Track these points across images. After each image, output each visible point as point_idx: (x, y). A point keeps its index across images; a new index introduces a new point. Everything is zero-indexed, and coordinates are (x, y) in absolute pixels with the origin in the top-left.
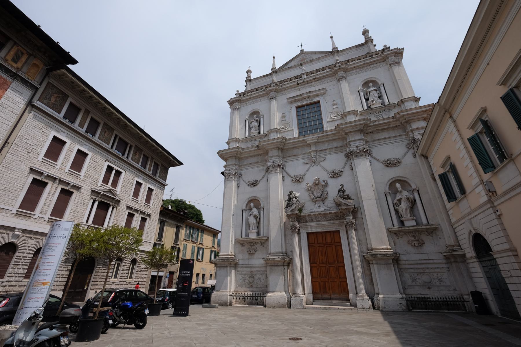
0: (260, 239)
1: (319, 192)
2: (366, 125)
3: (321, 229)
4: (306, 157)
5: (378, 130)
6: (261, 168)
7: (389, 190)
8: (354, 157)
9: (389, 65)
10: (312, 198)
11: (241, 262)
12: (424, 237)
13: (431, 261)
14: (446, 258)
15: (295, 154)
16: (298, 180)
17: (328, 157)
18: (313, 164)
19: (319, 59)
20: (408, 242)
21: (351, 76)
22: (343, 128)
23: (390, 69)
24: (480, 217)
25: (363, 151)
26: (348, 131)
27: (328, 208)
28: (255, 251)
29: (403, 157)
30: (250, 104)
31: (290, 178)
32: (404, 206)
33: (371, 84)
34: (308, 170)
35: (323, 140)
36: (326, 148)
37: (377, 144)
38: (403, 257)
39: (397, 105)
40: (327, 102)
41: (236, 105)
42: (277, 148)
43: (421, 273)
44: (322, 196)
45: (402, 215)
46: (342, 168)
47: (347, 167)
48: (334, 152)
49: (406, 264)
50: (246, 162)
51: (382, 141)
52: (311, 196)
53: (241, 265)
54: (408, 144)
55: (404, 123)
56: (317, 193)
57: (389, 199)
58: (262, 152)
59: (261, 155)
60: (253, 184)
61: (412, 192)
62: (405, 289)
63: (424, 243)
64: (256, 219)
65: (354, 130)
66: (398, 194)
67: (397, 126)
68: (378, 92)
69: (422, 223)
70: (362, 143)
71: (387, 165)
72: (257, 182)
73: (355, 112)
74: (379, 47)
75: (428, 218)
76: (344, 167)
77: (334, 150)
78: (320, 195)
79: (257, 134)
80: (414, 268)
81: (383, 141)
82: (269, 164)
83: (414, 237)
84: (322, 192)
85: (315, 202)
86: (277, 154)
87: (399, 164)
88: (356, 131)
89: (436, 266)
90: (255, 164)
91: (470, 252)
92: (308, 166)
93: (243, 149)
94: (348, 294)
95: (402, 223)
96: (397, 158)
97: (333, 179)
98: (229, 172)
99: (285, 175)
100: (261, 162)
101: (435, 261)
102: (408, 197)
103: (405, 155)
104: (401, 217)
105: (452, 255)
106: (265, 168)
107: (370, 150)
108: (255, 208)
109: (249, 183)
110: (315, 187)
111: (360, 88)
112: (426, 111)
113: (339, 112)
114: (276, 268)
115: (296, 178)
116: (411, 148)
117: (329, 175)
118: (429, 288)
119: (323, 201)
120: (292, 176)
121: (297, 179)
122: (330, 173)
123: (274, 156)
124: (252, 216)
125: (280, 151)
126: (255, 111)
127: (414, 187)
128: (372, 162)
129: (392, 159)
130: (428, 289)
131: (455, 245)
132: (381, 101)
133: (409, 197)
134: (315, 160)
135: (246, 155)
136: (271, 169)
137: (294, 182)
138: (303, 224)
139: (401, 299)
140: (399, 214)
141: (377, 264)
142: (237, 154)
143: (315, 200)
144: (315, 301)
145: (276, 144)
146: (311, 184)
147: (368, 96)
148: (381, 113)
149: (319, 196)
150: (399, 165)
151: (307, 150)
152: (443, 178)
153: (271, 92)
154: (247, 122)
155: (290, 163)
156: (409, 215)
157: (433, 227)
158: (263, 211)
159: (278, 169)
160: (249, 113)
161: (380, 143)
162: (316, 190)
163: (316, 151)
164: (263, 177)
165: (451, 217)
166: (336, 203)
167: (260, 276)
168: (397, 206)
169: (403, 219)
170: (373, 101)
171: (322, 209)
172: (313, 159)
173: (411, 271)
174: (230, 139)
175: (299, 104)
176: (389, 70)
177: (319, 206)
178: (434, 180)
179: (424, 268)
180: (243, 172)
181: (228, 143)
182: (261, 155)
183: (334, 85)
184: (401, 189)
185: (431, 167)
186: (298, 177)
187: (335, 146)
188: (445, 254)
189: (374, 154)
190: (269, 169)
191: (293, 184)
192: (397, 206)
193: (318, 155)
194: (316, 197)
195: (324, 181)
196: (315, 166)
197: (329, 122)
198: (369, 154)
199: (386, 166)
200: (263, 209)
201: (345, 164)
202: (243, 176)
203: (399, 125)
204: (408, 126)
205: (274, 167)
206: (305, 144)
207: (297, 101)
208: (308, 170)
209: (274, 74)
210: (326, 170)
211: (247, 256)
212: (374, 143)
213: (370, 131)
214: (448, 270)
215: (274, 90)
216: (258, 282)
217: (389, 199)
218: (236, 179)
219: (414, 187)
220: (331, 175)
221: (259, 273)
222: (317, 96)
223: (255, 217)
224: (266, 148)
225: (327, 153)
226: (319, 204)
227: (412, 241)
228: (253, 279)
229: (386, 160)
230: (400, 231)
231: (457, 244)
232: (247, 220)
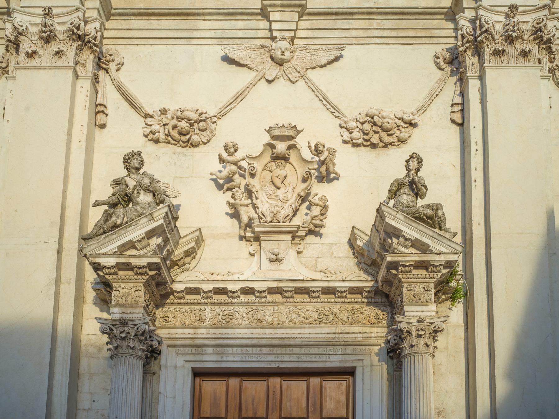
3: (271, 358)
4: (240, 34)
18: (272, 71)
31: (139, 121)
34: (240, 96)
46: (414, 110)
48: (387, 33)
76: (423, 109)
92: (246, 76)
115: (174, 122)
122: (353, 124)
137: (157, 141)
186: (179, 118)
196: (282, 83)
201: (434, 96)
208: (240, 96)
220: (356, 134)
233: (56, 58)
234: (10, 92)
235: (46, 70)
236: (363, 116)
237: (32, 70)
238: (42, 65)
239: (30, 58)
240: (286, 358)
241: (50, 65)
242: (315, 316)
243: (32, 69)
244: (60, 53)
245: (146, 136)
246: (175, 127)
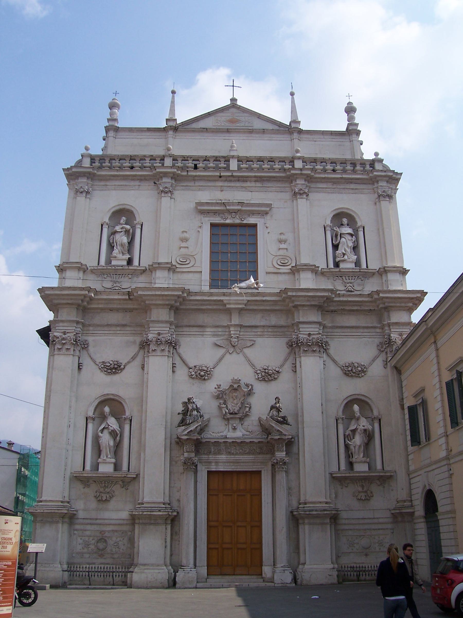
0: (123, 476)
1: (237, 404)
2: (328, 299)
3: (233, 467)
4: (220, 333)
5: (344, 310)
6: (131, 338)
7: (343, 415)
8: (302, 350)
9: (376, 195)
10: (224, 412)
11: (81, 514)
12: (374, 488)
13: (376, 521)
14: (394, 516)
15: (200, 323)
16: (201, 376)
17: (259, 340)
18: (231, 350)
19: (264, 131)
20: (354, 493)
21: (317, 192)
22: (293, 296)
23: (377, 203)
24: (436, 472)
25: (317, 344)
26: (299, 303)
27: (248, 433)
28: (111, 498)
29: (371, 364)
30: (115, 190)
32: (358, 440)
33: (345, 221)
34: (221, 359)
35: (255, 308)
36: (258, 324)
37: (338, 334)
38: (344, 515)
39: (378, 271)
40: (268, 233)
41: (83, 182)
42: (168, 305)
43: (360, 536)
44: (241, 411)
45: (353, 454)
47: (288, 366)
48: (270, 333)
49: (345, 524)
50: (97, 320)
51: (346, 330)
52: (223, 409)
53: (81, 521)
54: (381, 343)
55: (382, 308)
56: (233, 405)
57: (341, 427)
58: (135, 307)
59: (131, 310)
60: (111, 369)
61: (372, 420)
62: (338, 557)
63: (373, 496)
64: (115, 439)
65: (308, 303)
66: (353, 422)
67: (370, 310)
68: (354, 240)
69: (376, 469)
70: (317, 330)
71: (347, 372)
72: (120, 366)
73: (314, 270)
74: (368, 155)
75: (384, 461)
76: (282, 366)
77: (270, 330)
78: (238, 408)
79: (125, 263)
80: (354, 529)
81: (349, 330)
82: (150, 336)
83: (363, 487)
84: (242, 403)
85: (228, 419)
86: (167, 319)
87: (363, 374)
88: (311, 306)
89: (380, 526)
90: (118, 328)
91: (420, 510)
92: (222, 351)
93: (96, 292)
94: (261, 566)
95: (351, 465)
96: (363, 364)
97: (263, 383)
98: (64, 336)
99: (178, 361)
100: (130, 326)
101: (381, 520)
102: (365, 427)
103: (374, 360)
104: (351, 456)
105: (401, 513)
106: (138, 339)
107: (327, 342)
108: (113, 416)
109: (102, 366)
110: (231, 394)
111: (328, 222)
112: (412, 298)
113: (288, 258)
114: (152, 527)
115: (199, 372)
116: (383, 351)
117: (257, 376)
118: (366, 555)
119: (241, 419)
120: (191, 365)
121: (199, 373)
122: (259, 372)
123: (162, 322)
124: (106, 431)
125: (172, 312)
126: (124, 209)
127: (376, 413)
128: (326, 363)
129: (356, 365)
130: (365, 557)
131: (408, 500)
132: (356, 257)
133: (367, 428)
134: (236, 343)
135: (100, 306)
136: (152, 347)
137: (193, 378)
138: (204, 457)
139: (331, 570)
140: (350, 452)
141: (310, 524)
142: (82, 301)
143: (229, 416)
144: (209, 577)
145: (168, 298)
146: (225, 386)
147: (337, 242)
148: (353, 281)
149: (236, 411)
150: (362, 376)
151: (223, 320)
152: (413, 410)
153: (164, 176)
154: (105, 230)
155: (188, 339)
156: (362, 455)
157: (387, 474)
158: (129, 425)
159: (167, 349)
160: (112, 211)
161: (343, 334)
162: (231, 400)
163: (241, 326)
164: (133, 358)
165: (410, 462)
166: (261, 425)
167: (118, 539)
168: (348, 440)
169: (354, 460)
170: (344, 254)
171: (238, 434)
172: (234, 340)
173: (350, 533)
174: (67, 263)
175: (218, 220)
176: (376, 203)
177: (235, 429)
178: (403, 408)
179: (365, 530)
180: (90, 339)
181: (61, 269)
182: (131, 310)
183: (286, 202)
184: (359, 414)
185: (402, 388)
187: (273, 323)
188: (393, 512)
189: (331, 351)
190: (149, 345)
191: (191, 380)
192: (349, 439)
193: (241, 334)
194: (232, 411)
195: (247, 385)
197: (269, 273)
198: (325, 349)
199: (345, 374)
200: (129, 422)
201: (286, 360)
202: (91, 349)
203: (374, 310)
204: (386, 314)
205: (158, 342)
206: (221, 307)
207: (215, 213)
208: (221, 359)
209: (171, 133)
210: (253, 366)
211: (93, 504)
212: (335, 330)
213: (332, 308)
214: (392, 531)
215: (172, 175)
216: (114, 550)
217: (341, 427)
218: (77, 353)
219: (376, 413)
220: (260, 376)
221: (116, 534)
222: (252, 213)
223: (113, 434)
224: (147, 302)
225: (259, 333)
226: (235, 425)
227: (359, 492)
228: (104, 544)
229: (347, 364)
230: (346, 478)
231: (410, 499)
232: (96, 439)
236: (262, 369)
240: (238, 467)
242: (248, 451)
245: (190, 376)
246: (199, 373)
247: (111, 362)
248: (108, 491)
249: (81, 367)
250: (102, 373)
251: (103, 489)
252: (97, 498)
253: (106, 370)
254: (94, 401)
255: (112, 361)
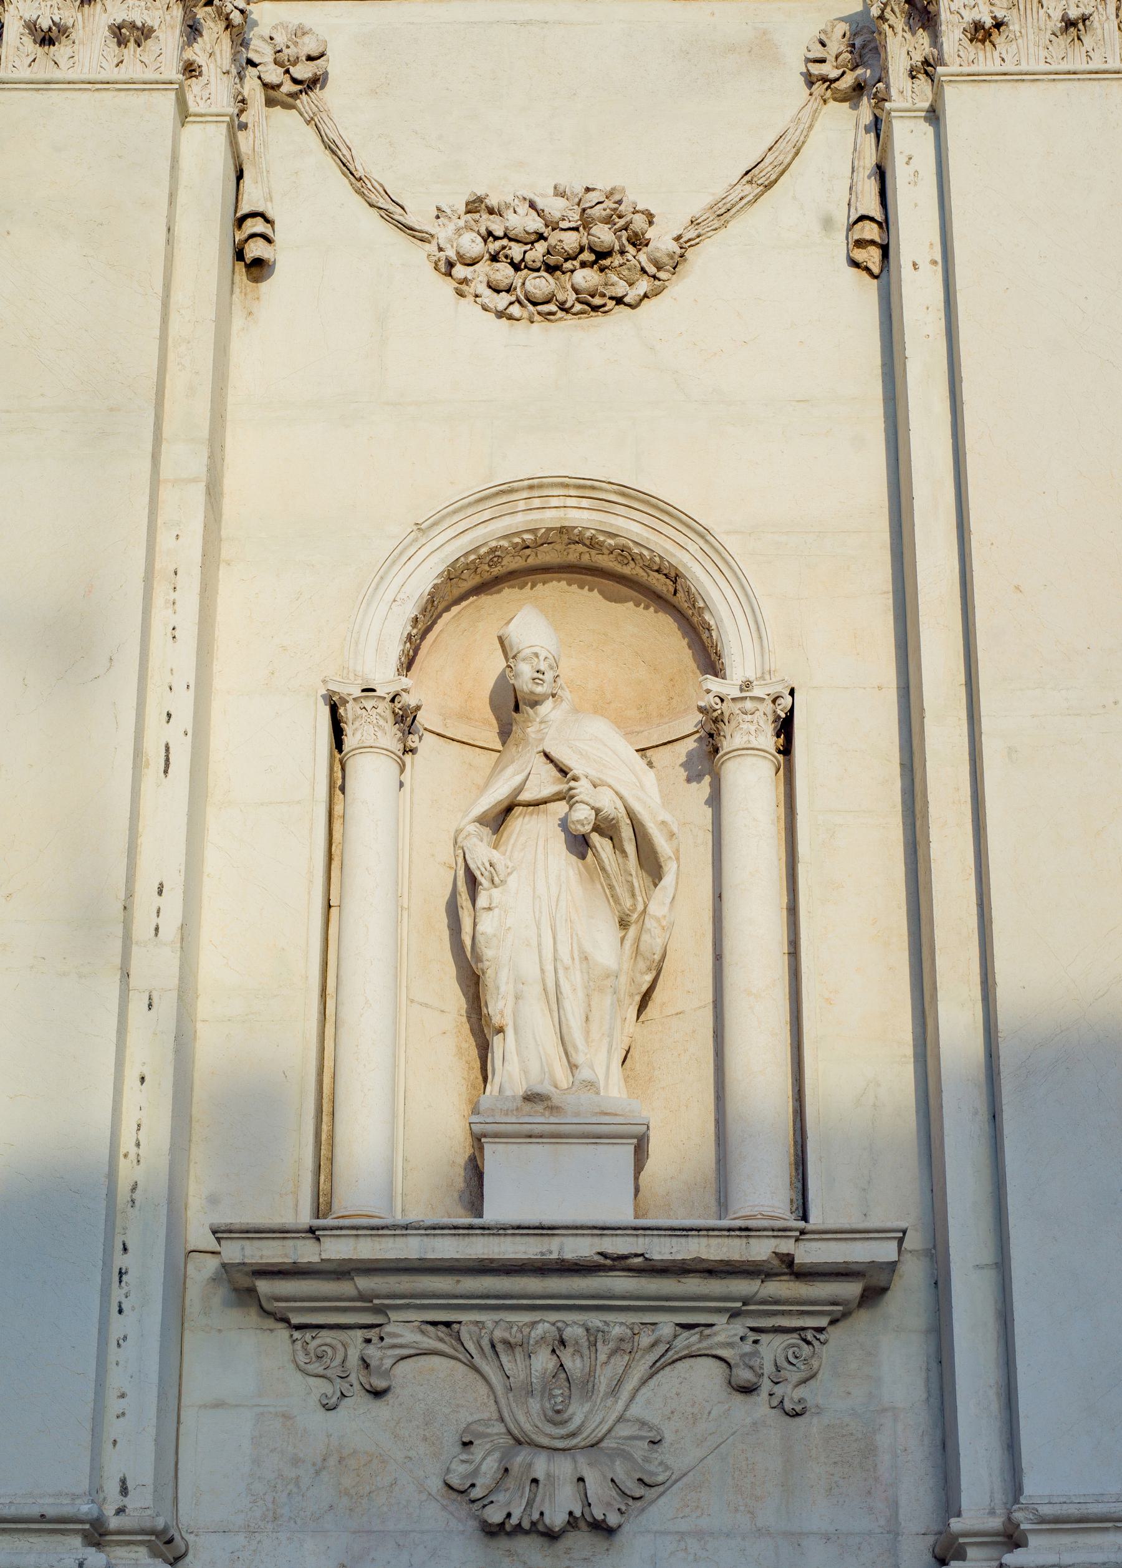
200: (768, 741)
233: (1063, 41)
234: (907, 163)
235: (1039, 83)
237: (993, 85)
238: (1024, 67)
239: (979, 44)
241: (1048, 68)
243: (996, 81)
244: (1081, 26)
247: (555, 207)
248: (595, 1427)
249: (255, 249)
250: (467, 303)
251: (535, 1405)
252: (484, 1502)
253: (503, 272)
254: (397, 556)
255: (560, 193)
